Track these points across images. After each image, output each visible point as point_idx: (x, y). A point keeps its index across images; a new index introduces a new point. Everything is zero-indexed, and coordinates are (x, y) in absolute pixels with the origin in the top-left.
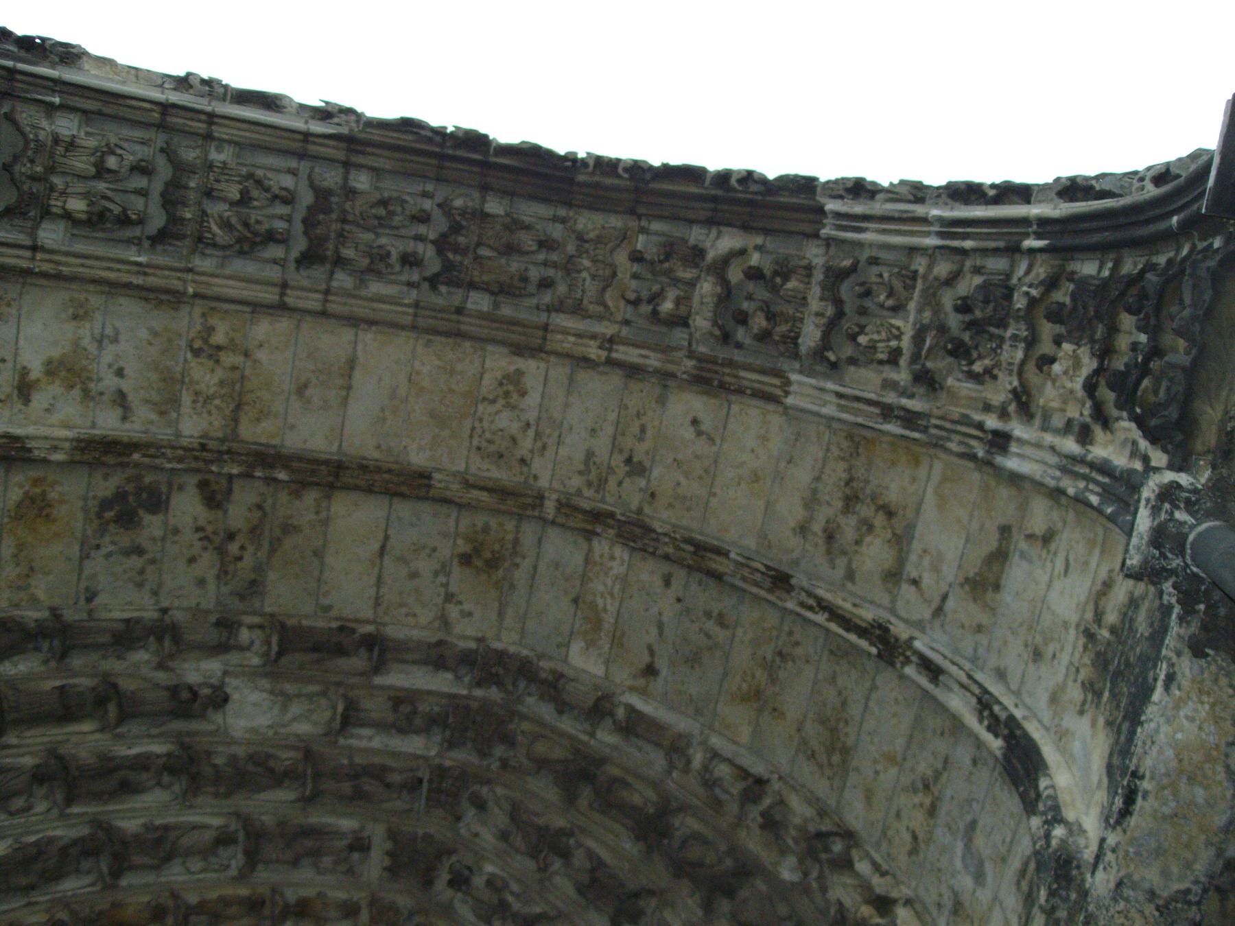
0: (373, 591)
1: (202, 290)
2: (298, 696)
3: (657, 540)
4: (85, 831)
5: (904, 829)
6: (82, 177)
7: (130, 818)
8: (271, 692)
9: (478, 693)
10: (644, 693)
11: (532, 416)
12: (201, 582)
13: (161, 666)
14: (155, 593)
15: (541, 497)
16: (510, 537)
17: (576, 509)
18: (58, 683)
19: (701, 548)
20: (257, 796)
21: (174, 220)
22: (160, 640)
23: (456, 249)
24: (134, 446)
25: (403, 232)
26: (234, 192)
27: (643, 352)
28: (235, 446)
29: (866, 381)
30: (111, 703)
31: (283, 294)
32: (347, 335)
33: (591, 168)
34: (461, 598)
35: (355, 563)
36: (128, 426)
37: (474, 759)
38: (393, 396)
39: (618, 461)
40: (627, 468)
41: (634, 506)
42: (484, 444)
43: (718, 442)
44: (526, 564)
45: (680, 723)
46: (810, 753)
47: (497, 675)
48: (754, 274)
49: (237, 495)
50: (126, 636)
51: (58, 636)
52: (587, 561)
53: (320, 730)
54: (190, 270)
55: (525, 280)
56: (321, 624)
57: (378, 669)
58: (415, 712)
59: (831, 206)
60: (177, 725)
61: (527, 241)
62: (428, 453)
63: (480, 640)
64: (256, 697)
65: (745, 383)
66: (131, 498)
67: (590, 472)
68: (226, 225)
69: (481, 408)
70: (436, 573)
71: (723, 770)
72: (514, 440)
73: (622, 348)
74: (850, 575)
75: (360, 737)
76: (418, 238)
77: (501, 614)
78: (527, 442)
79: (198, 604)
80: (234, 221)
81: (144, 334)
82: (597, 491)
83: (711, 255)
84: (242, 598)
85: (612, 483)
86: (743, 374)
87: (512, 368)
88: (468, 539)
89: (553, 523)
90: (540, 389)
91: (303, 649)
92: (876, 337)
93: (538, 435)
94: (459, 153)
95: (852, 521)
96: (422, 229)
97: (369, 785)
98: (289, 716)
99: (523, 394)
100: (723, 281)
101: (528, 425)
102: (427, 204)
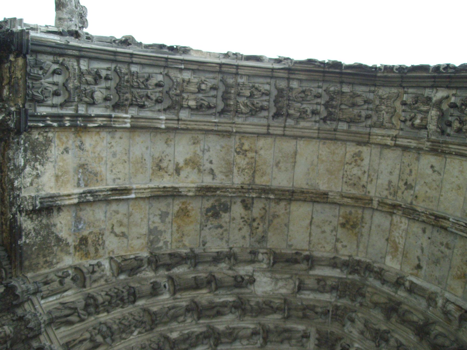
0: (308, 239)
1: (239, 130)
2: (281, 279)
3: (419, 215)
4: (204, 329)
6: (193, 93)
7: (221, 325)
8: (271, 278)
9: (350, 277)
10: (416, 276)
11: (366, 169)
12: (244, 237)
13: (230, 269)
14: (227, 242)
15: (372, 200)
16: (360, 216)
17: (386, 204)
18: (193, 275)
19: (437, 217)
20: (266, 317)
21: (227, 105)
22: (229, 259)
23: (332, 107)
24: (217, 189)
25: (312, 102)
26: (248, 93)
27: (409, 140)
28: (254, 186)
30: (212, 283)
31: (268, 129)
32: (293, 142)
33: (382, 71)
34: (342, 240)
35: (300, 229)
36: (215, 181)
37: (349, 302)
38: (312, 164)
39: (401, 184)
40: (406, 187)
41: (409, 201)
42: (348, 181)
43: (442, 174)
44: (367, 226)
47: (357, 270)
49: (255, 205)
50: (217, 259)
51: (193, 259)
52: (391, 224)
53: (290, 292)
54: (234, 123)
55: (360, 116)
56: (289, 252)
57: (311, 268)
58: (326, 284)
60: (237, 291)
61: (359, 101)
62: (326, 185)
63: (350, 256)
64: (265, 279)
66: (217, 207)
67: (390, 189)
68: (246, 105)
69: (346, 166)
70: (332, 231)
72: (360, 178)
73: (400, 140)
75: (304, 294)
76: (317, 104)
77: (358, 246)
78: (365, 179)
79: (243, 246)
80: (249, 104)
81: (218, 147)
82: (394, 196)
84: (259, 243)
85: (400, 193)
87: (357, 150)
88: (344, 217)
89: (377, 210)
90: (369, 157)
91: (282, 261)
93: (369, 176)
94: (331, 70)
96: (319, 100)
97: (309, 313)
98: (278, 286)
99: (362, 160)
100: (440, 110)
101: (365, 172)
102: (320, 91)
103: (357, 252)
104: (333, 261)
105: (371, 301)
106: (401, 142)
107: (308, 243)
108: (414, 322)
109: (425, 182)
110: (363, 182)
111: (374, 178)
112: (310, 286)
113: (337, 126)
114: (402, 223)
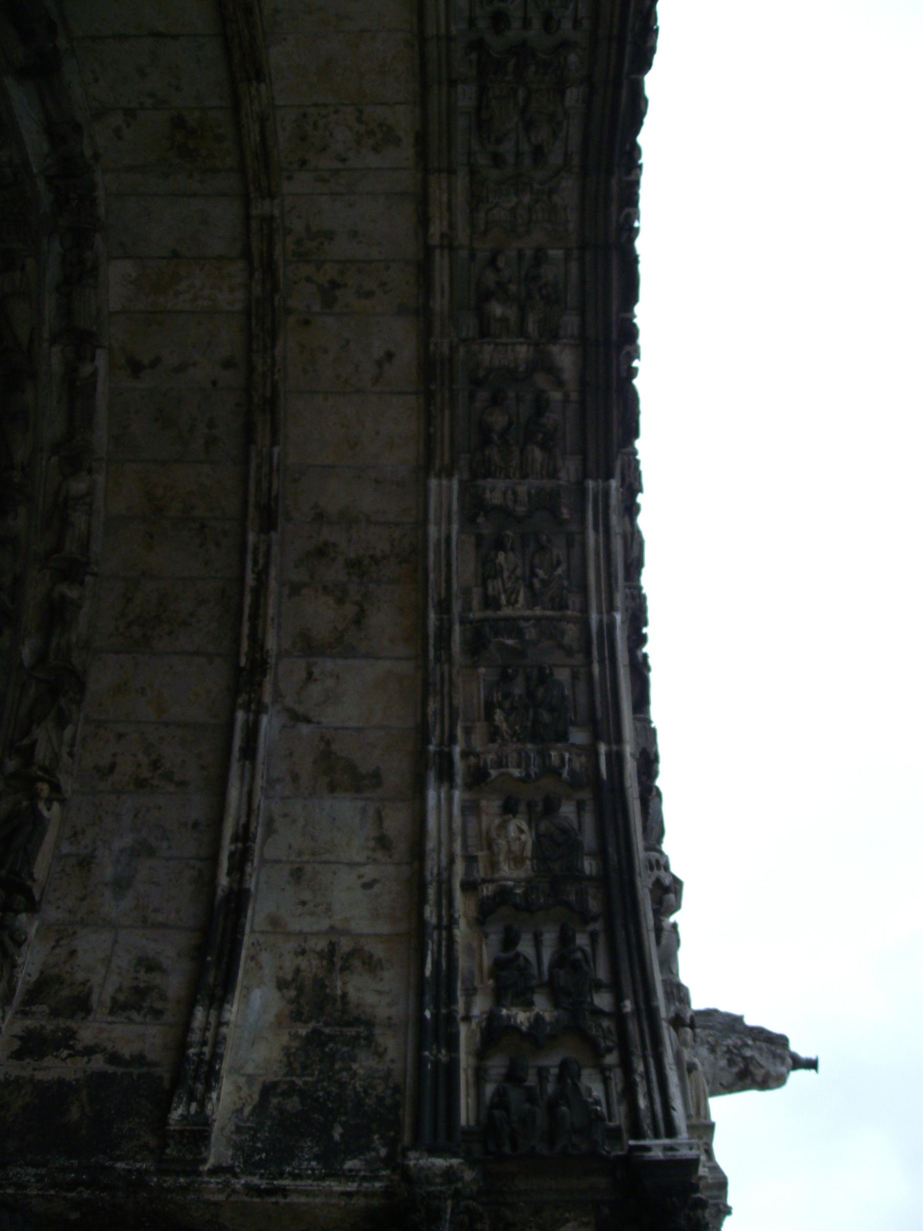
15: (272, 196)
19: (272, 404)
29: (465, 569)
40: (326, 285)
45: (100, 438)
48: (541, 405)
55: (499, 141)
59: (614, 484)
63: (96, 157)
72: (324, 149)
73: (446, 262)
74: (295, 589)
83: (555, 349)
86: (447, 413)
89: (248, 218)
92: (506, 574)
93: (336, 172)
99: (376, 149)
101: (344, 160)
106: (441, 261)
109: (348, 342)
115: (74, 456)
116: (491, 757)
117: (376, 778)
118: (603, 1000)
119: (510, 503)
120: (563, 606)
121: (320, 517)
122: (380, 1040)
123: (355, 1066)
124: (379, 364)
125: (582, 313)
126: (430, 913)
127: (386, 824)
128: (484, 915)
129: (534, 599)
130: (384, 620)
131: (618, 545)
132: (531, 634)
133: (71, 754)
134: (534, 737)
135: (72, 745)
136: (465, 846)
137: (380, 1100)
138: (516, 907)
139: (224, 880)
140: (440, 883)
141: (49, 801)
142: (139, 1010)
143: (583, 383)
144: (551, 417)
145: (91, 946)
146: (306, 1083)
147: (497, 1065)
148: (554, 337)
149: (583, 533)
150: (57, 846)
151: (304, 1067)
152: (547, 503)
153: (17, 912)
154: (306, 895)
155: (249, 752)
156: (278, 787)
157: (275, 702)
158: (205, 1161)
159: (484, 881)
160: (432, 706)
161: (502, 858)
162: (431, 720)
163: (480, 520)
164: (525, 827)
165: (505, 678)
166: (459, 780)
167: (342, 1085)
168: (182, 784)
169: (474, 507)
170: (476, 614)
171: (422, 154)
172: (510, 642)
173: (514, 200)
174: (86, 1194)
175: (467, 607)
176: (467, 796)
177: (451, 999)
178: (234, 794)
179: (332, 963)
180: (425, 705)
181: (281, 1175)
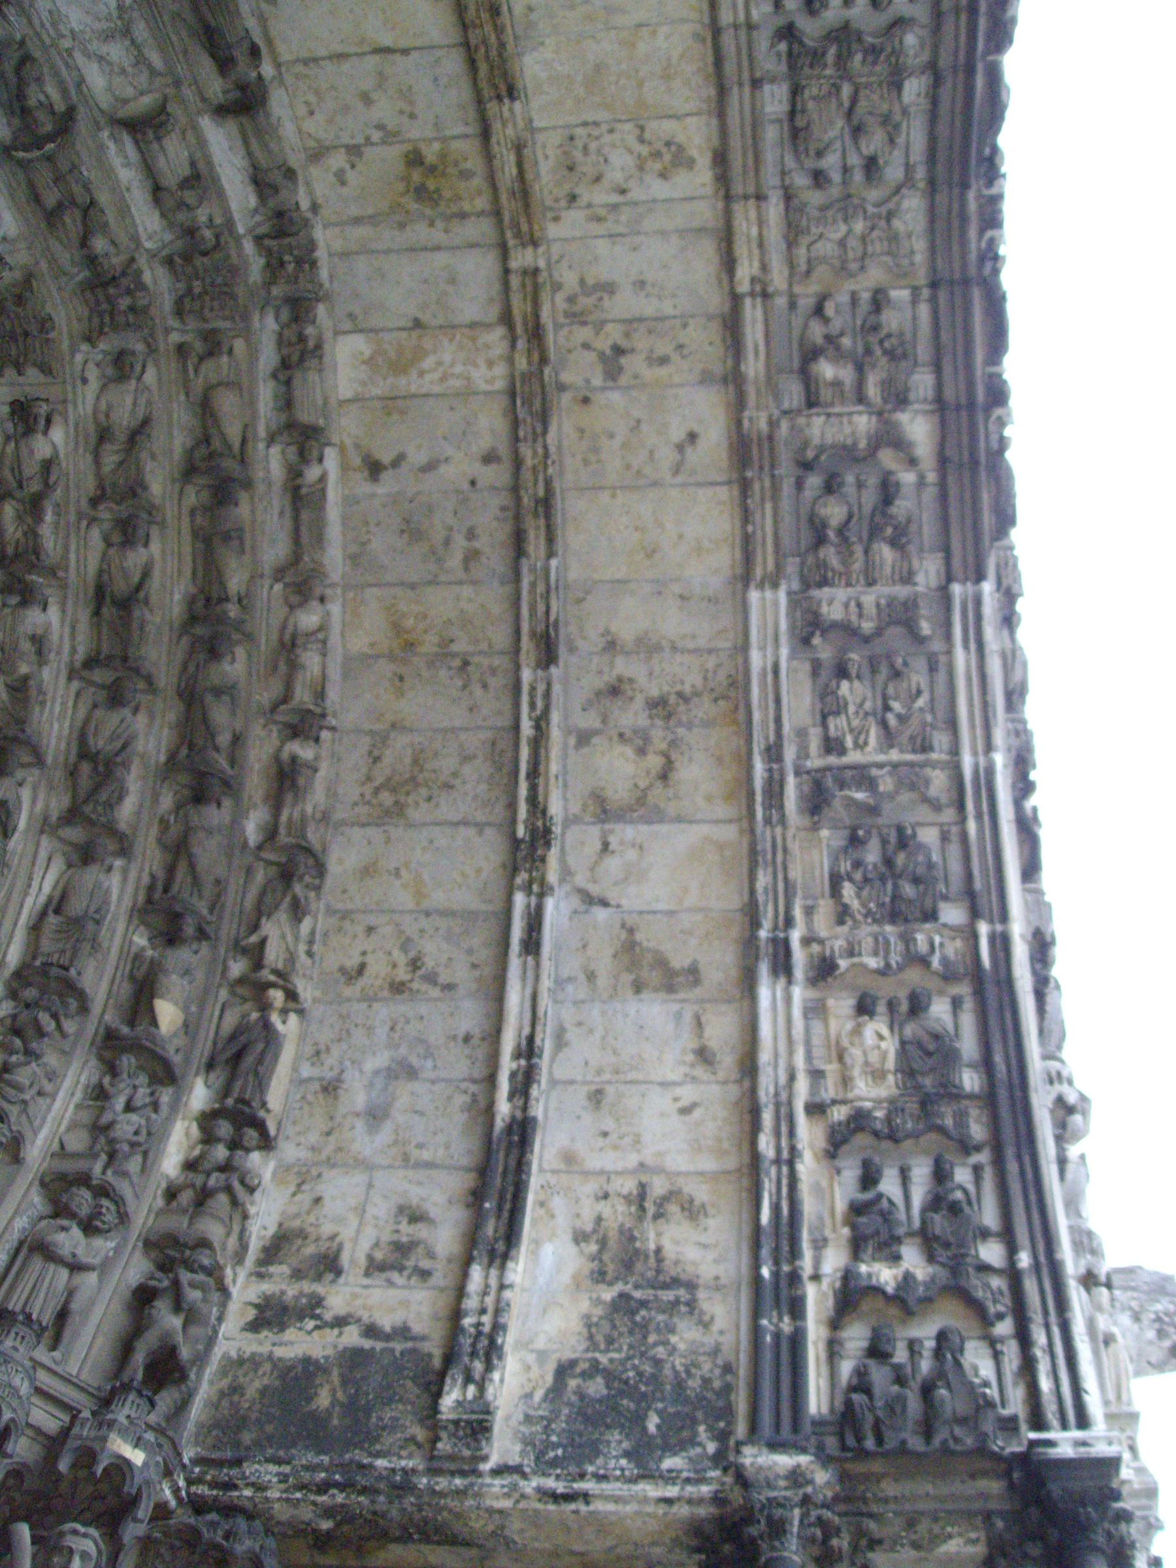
0: (322, 52)
5: (361, 949)
9: (249, 247)
11: (636, 194)
15: (535, 243)
16: (467, 207)
17: (536, 304)
19: (546, 504)
27: (762, 349)
29: (799, 704)
33: (986, 192)
34: (360, 167)
39: (614, 334)
40: (608, 352)
41: (566, 377)
42: (579, 143)
43: (680, 479)
44: (437, 235)
45: (334, 558)
46: (376, 753)
47: (282, 264)
48: (888, 491)
52: (473, 325)
55: (819, 154)
59: (987, 587)
61: (874, 142)
62: (543, 75)
65: (758, 516)
67: (589, 295)
69: (628, 127)
70: (380, 127)
71: (311, 660)
72: (598, 179)
74: (584, 738)
77: (357, 221)
78: (601, 197)
82: (567, 314)
83: (903, 417)
85: (584, 333)
86: (768, 506)
87: (694, 153)
88: (443, 156)
89: (507, 271)
90: (676, 195)
92: (851, 709)
93: (614, 207)
95: (643, 721)
98: (104, 49)
99: (663, 175)
100: (877, 442)
101: (623, 192)
103: (336, 225)
104: (277, 177)
105: (208, 390)
106: (752, 313)
107: (304, 54)
108: (222, 585)
109: (639, 421)
110: (586, 195)
111: (610, 226)
112: (162, 163)
113: (773, 80)
114: (489, 376)
115: (302, 583)
116: (839, 944)
117: (693, 973)
118: (991, 1253)
119: (854, 618)
120: (926, 748)
121: (611, 646)
122: (705, 1305)
123: (674, 1339)
124: (680, 448)
125: (937, 367)
126: (766, 1144)
127: (708, 1031)
128: (836, 1144)
129: (889, 738)
130: (699, 774)
131: (995, 666)
132: (886, 784)
133: (310, 954)
134: (894, 915)
135: (311, 942)
136: (809, 1057)
137: (706, 1381)
138: (876, 1134)
139: (504, 1108)
140: (777, 1105)
141: (284, 1012)
142: (401, 1269)
143: (943, 461)
144: (902, 507)
145: (340, 1191)
146: (611, 1360)
147: (856, 1336)
148: (901, 400)
149: (949, 652)
150: (295, 1069)
151: (610, 1341)
152: (902, 615)
153: (248, 1150)
154: (609, 1124)
155: (532, 945)
156: (570, 988)
157: (562, 881)
158: (485, 1458)
159: (834, 1102)
160: (763, 880)
161: (856, 1072)
162: (761, 898)
163: (816, 640)
164: (885, 1031)
165: (855, 841)
166: (799, 973)
167: (658, 1363)
168: (449, 987)
169: (809, 626)
170: (815, 761)
171: (723, 178)
172: (860, 796)
173: (843, 228)
174: (340, 1498)
175: (803, 753)
176: (812, 994)
177: (795, 1253)
178: (515, 998)
179: (642, 1208)
180: (752, 879)
181: (582, 1476)
